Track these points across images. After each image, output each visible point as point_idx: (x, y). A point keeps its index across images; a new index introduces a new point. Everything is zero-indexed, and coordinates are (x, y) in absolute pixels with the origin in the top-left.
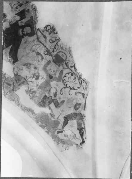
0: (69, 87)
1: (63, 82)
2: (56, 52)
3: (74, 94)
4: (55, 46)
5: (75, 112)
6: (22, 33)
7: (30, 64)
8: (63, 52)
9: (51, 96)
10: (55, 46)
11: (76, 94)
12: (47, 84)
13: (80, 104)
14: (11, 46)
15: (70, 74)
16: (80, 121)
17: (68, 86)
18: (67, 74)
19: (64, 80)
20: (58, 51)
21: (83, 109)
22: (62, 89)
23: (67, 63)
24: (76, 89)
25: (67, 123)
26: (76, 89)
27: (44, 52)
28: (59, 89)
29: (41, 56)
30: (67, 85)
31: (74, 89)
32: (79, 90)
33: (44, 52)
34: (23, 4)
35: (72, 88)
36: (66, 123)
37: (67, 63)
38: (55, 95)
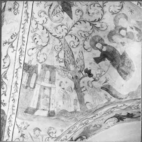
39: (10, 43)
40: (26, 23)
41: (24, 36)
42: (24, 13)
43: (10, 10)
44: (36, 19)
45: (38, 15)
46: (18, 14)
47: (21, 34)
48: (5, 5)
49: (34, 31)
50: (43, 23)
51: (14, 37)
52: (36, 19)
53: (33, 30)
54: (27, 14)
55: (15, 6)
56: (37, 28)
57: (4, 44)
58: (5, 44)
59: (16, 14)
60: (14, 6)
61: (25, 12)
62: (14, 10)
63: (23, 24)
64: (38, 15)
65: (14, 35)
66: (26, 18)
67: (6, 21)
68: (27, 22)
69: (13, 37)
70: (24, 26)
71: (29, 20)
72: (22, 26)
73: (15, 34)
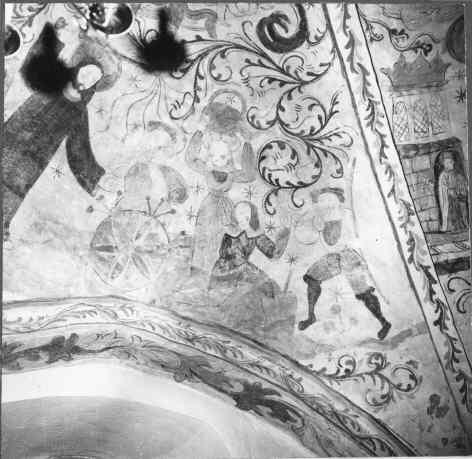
0: (288, 183)
1: (264, 178)
2: (208, 97)
3: (308, 200)
4: (195, 83)
5: (332, 249)
6: (79, 92)
7: (145, 166)
8: (226, 91)
9: (244, 232)
10: (195, 83)
11: (314, 198)
12: (218, 197)
13: (337, 223)
14: (64, 143)
15: (275, 145)
16: (358, 272)
17: (282, 183)
18: (267, 150)
19: (264, 169)
20: (210, 94)
21: (354, 235)
22: (267, 199)
23: (253, 117)
24: (311, 184)
25: (318, 291)
26: (311, 184)
27: (170, 114)
28: (258, 202)
29: (167, 129)
30: (277, 180)
31: (303, 185)
32: (318, 186)
33: (170, 114)
34: (34, 16)
35: (295, 184)
36: (314, 293)
37: (253, 117)
38: (255, 223)
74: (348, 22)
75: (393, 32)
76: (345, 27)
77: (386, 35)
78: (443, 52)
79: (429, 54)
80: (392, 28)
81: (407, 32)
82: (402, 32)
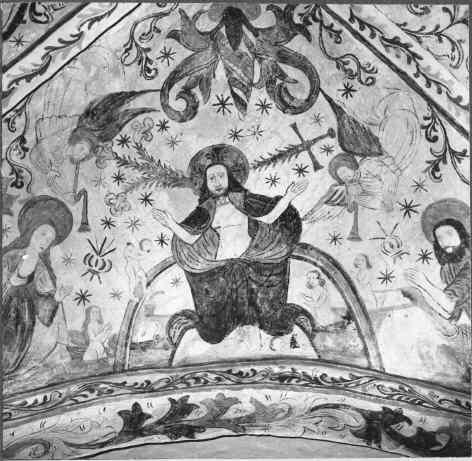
39: (445, 152)
40: (419, 61)
41: (454, 96)
42: (388, 51)
43: (348, 91)
44: (423, 28)
45: (416, 14)
46: (377, 77)
47: (442, 101)
48: (325, 96)
49: (456, 60)
50: (450, 13)
51: (436, 131)
52: (423, 28)
53: (453, 59)
54: (395, 42)
55: (347, 67)
56: (453, 42)
57: (437, 174)
58: (438, 170)
59: (370, 81)
60: (345, 71)
61: (386, 46)
62: (356, 80)
63: (416, 75)
64: (416, 14)
65: (426, 127)
66: (404, 56)
67: (371, 124)
68: (421, 58)
69: (433, 134)
70: (424, 75)
71: (416, 48)
72: (421, 82)
73: (427, 123)
74: (23, 82)
75: (22, 139)
76: (17, 81)
77: (18, 134)
78: (21, 202)
79: (14, 188)
80: (26, 137)
81: (27, 154)
82: (26, 150)
